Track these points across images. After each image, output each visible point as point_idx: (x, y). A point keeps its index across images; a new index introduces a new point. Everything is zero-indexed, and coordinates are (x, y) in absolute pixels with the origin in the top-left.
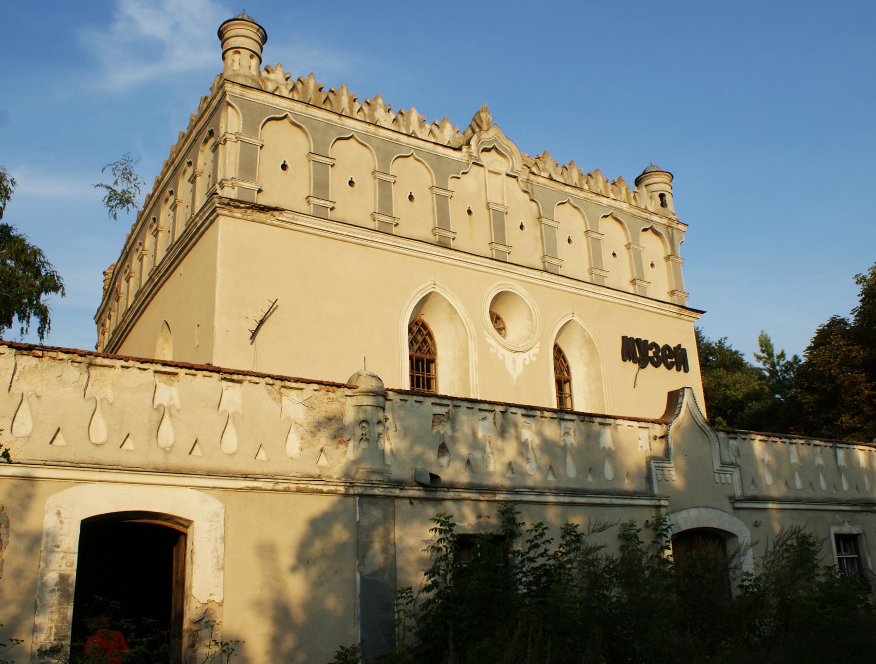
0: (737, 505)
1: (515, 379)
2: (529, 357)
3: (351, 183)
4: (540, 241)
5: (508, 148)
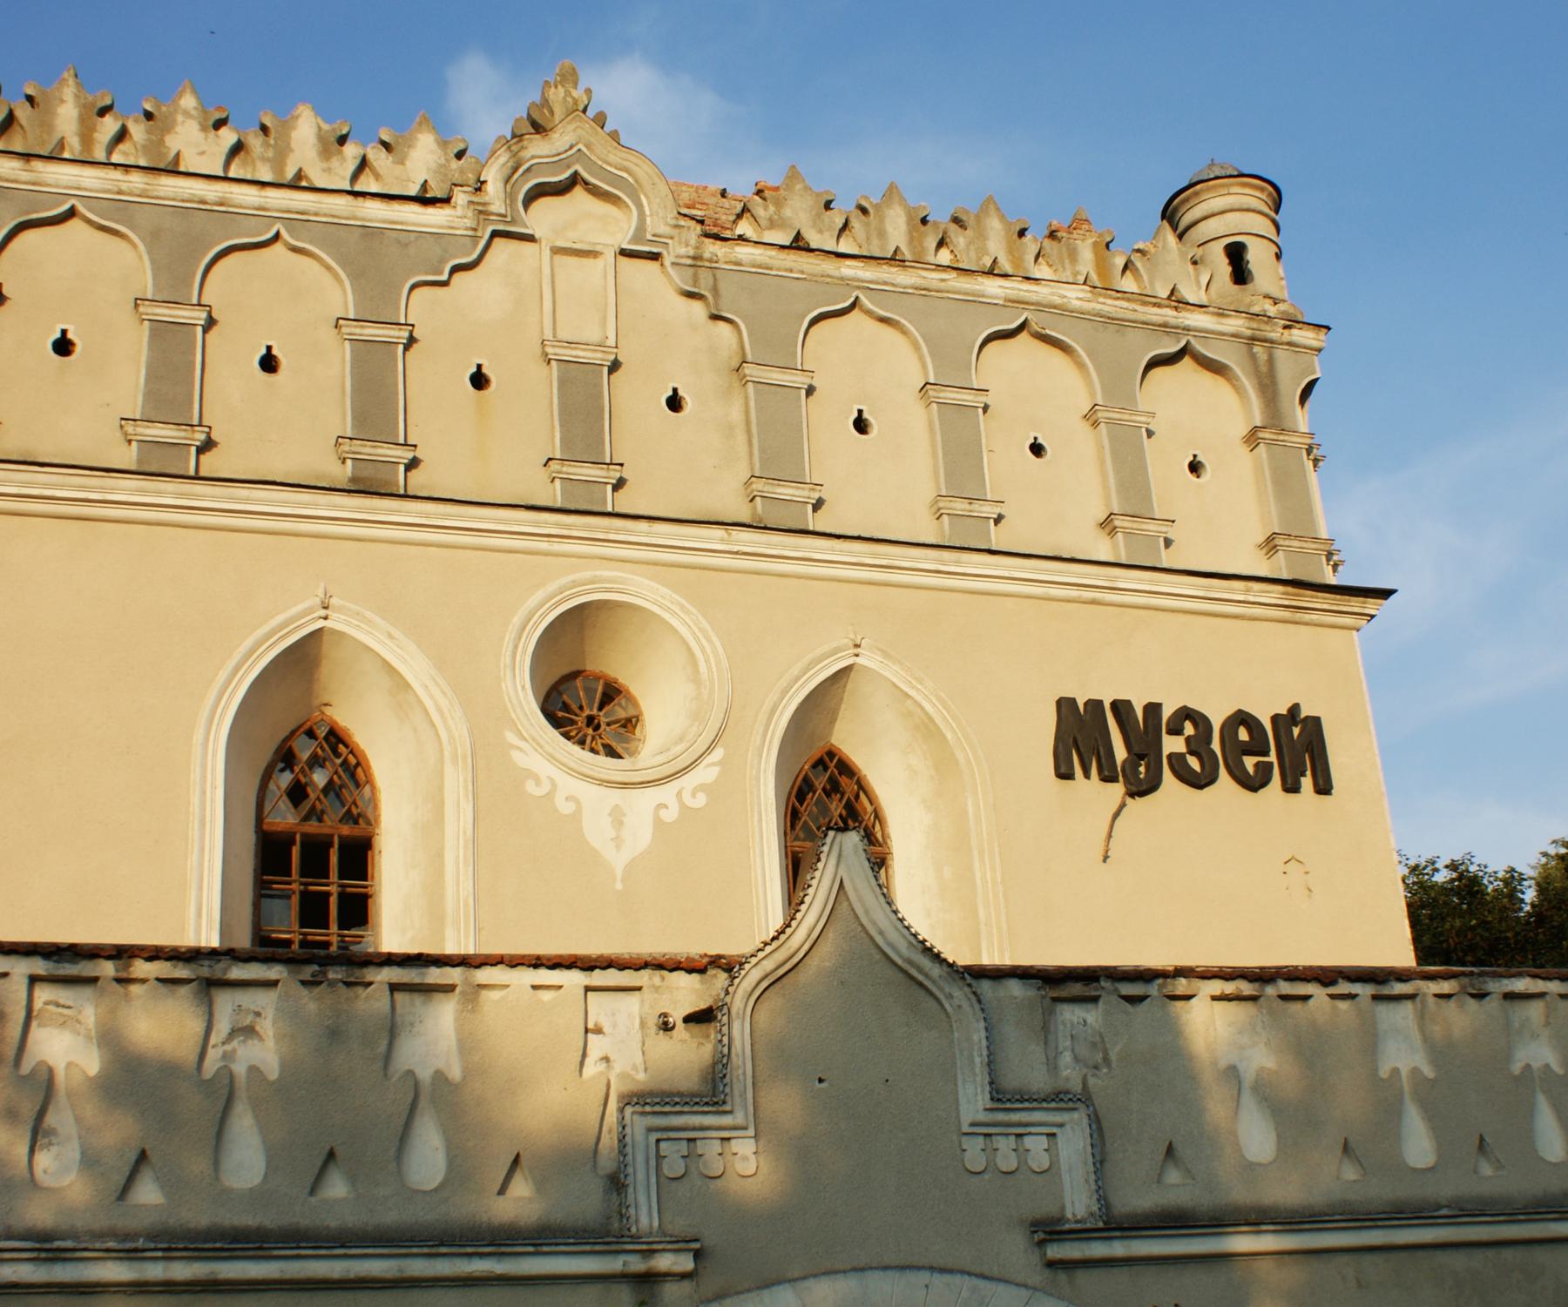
0: (1055, 1251)
1: (619, 873)
2: (679, 794)
4: (741, 438)
5: (625, 175)
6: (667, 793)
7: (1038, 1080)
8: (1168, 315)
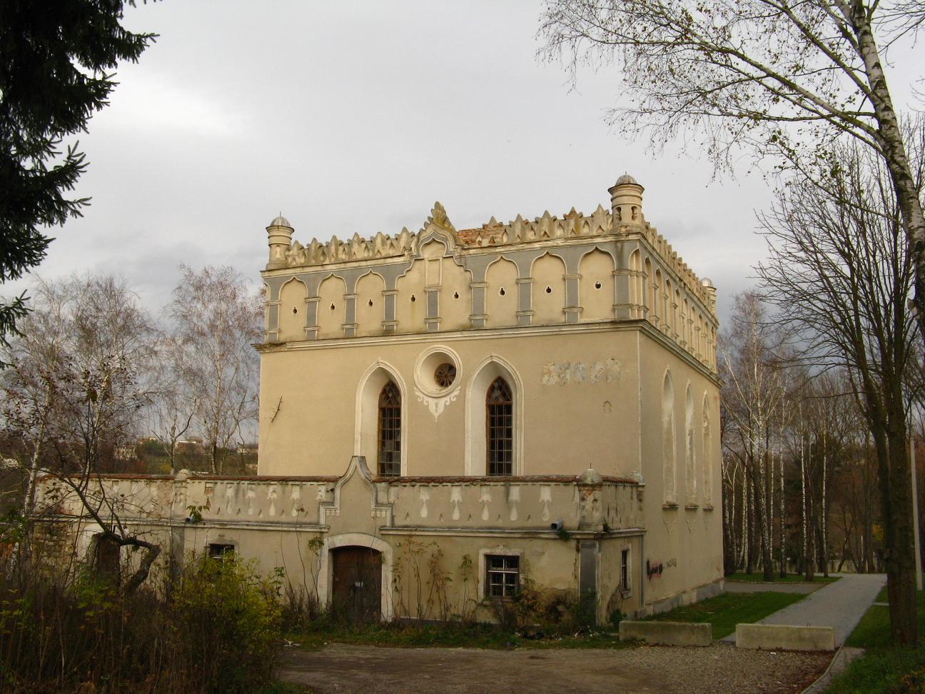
0: (382, 532)
3: (333, 307)
6: (447, 399)
7: (385, 501)
8: (589, 241)
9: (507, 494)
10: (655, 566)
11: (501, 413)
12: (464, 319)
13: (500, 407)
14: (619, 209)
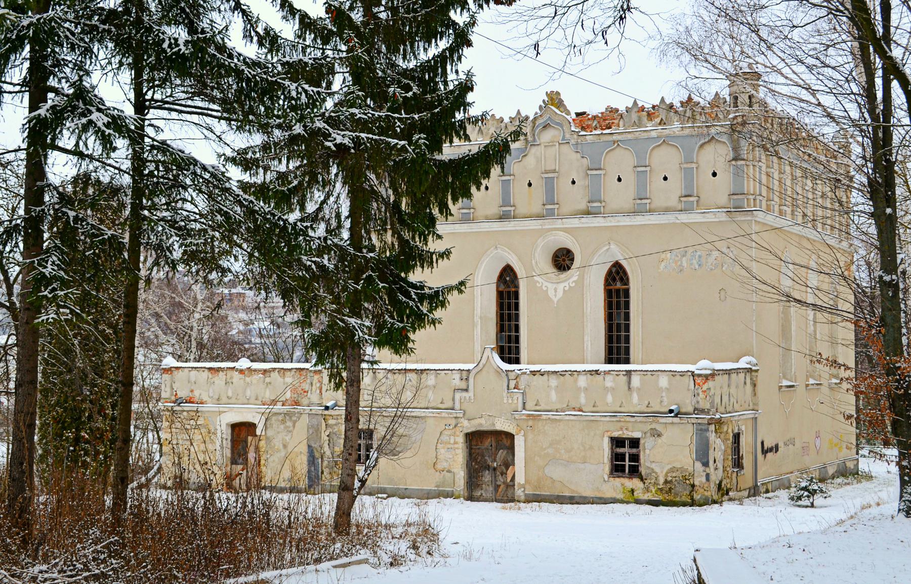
6: (566, 284)
9: (629, 383)
10: (770, 446)
11: (618, 296)
12: (583, 206)
13: (618, 291)
14: (736, 98)
